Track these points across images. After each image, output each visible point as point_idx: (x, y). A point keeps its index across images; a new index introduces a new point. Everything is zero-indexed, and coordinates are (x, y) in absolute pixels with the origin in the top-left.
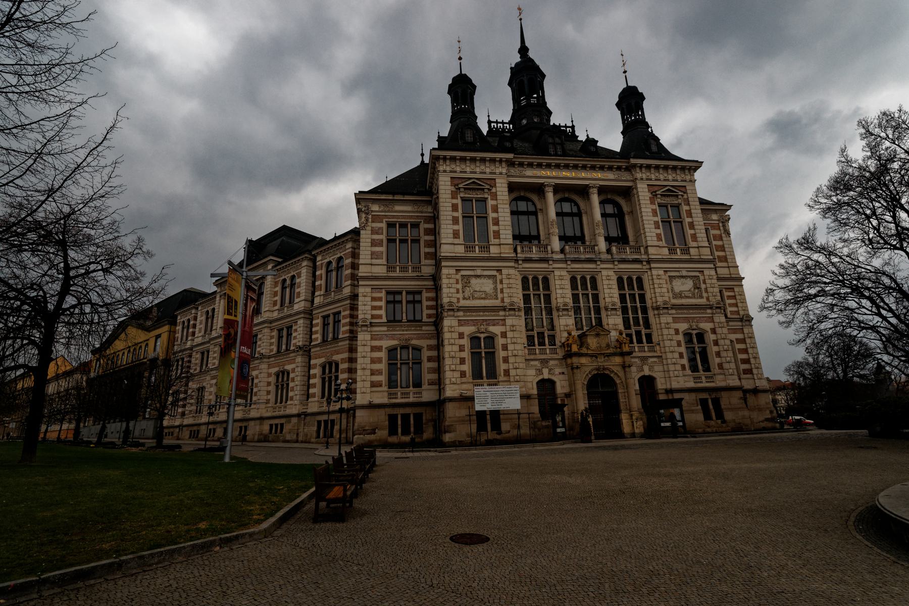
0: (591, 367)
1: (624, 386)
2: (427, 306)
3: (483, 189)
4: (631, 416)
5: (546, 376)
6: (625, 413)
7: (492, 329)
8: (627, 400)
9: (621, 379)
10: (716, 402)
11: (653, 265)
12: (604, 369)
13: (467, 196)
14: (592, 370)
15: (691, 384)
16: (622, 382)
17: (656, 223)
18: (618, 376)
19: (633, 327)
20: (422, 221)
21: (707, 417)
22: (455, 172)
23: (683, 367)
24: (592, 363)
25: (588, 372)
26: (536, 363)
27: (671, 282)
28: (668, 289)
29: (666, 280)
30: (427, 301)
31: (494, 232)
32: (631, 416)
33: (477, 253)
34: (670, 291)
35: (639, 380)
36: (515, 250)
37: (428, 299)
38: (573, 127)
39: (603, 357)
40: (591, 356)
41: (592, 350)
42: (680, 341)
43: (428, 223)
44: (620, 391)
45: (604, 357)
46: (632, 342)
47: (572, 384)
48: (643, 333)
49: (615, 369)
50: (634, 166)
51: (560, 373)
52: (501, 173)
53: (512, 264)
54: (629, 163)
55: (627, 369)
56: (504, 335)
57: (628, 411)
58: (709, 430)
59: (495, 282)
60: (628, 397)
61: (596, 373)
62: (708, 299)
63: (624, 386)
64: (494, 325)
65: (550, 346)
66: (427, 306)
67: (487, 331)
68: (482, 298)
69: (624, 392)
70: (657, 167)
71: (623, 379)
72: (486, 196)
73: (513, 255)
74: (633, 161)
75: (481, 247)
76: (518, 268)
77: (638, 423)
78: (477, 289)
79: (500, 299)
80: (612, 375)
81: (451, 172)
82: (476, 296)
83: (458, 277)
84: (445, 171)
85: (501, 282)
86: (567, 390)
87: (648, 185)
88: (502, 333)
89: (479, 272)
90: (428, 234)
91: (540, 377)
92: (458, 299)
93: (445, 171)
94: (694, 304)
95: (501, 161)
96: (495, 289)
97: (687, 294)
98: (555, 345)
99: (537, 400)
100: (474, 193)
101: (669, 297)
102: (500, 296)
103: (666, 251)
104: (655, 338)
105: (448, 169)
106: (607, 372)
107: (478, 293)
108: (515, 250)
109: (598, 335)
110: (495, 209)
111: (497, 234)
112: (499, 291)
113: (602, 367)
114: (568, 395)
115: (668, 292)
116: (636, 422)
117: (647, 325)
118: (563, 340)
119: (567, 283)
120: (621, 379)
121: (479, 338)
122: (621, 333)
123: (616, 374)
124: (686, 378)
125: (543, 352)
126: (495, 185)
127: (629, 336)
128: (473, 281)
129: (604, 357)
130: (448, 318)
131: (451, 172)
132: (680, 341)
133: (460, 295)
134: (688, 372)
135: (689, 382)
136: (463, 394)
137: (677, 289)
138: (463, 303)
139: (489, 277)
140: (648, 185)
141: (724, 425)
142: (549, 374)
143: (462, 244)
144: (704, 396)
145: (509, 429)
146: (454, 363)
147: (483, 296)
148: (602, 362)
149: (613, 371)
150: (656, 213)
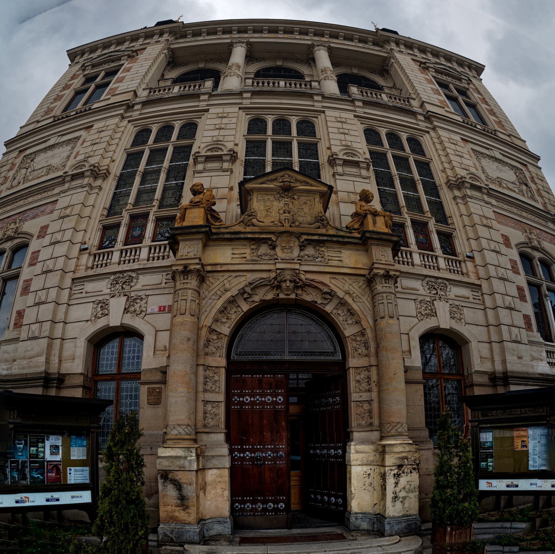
0: (250, 277)
1: (367, 348)
4: (382, 451)
6: (363, 442)
8: (374, 395)
9: (358, 322)
14: (255, 286)
16: (363, 333)
18: (351, 312)
24: (254, 262)
25: (234, 292)
32: (382, 451)
39: (295, 244)
44: (353, 362)
45: (302, 247)
55: (380, 287)
57: (375, 435)
60: (379, 384)
61: (270, 296)
63: (367, 348)
69: (368, 368)
71: (368, 322)
80: (328, 308)
106: (309, 297)
113: (288, 276)
120: (358, 322)
123: (342, 303)
129: (302, 247)
148: (290, 261)
149: (331, 294)
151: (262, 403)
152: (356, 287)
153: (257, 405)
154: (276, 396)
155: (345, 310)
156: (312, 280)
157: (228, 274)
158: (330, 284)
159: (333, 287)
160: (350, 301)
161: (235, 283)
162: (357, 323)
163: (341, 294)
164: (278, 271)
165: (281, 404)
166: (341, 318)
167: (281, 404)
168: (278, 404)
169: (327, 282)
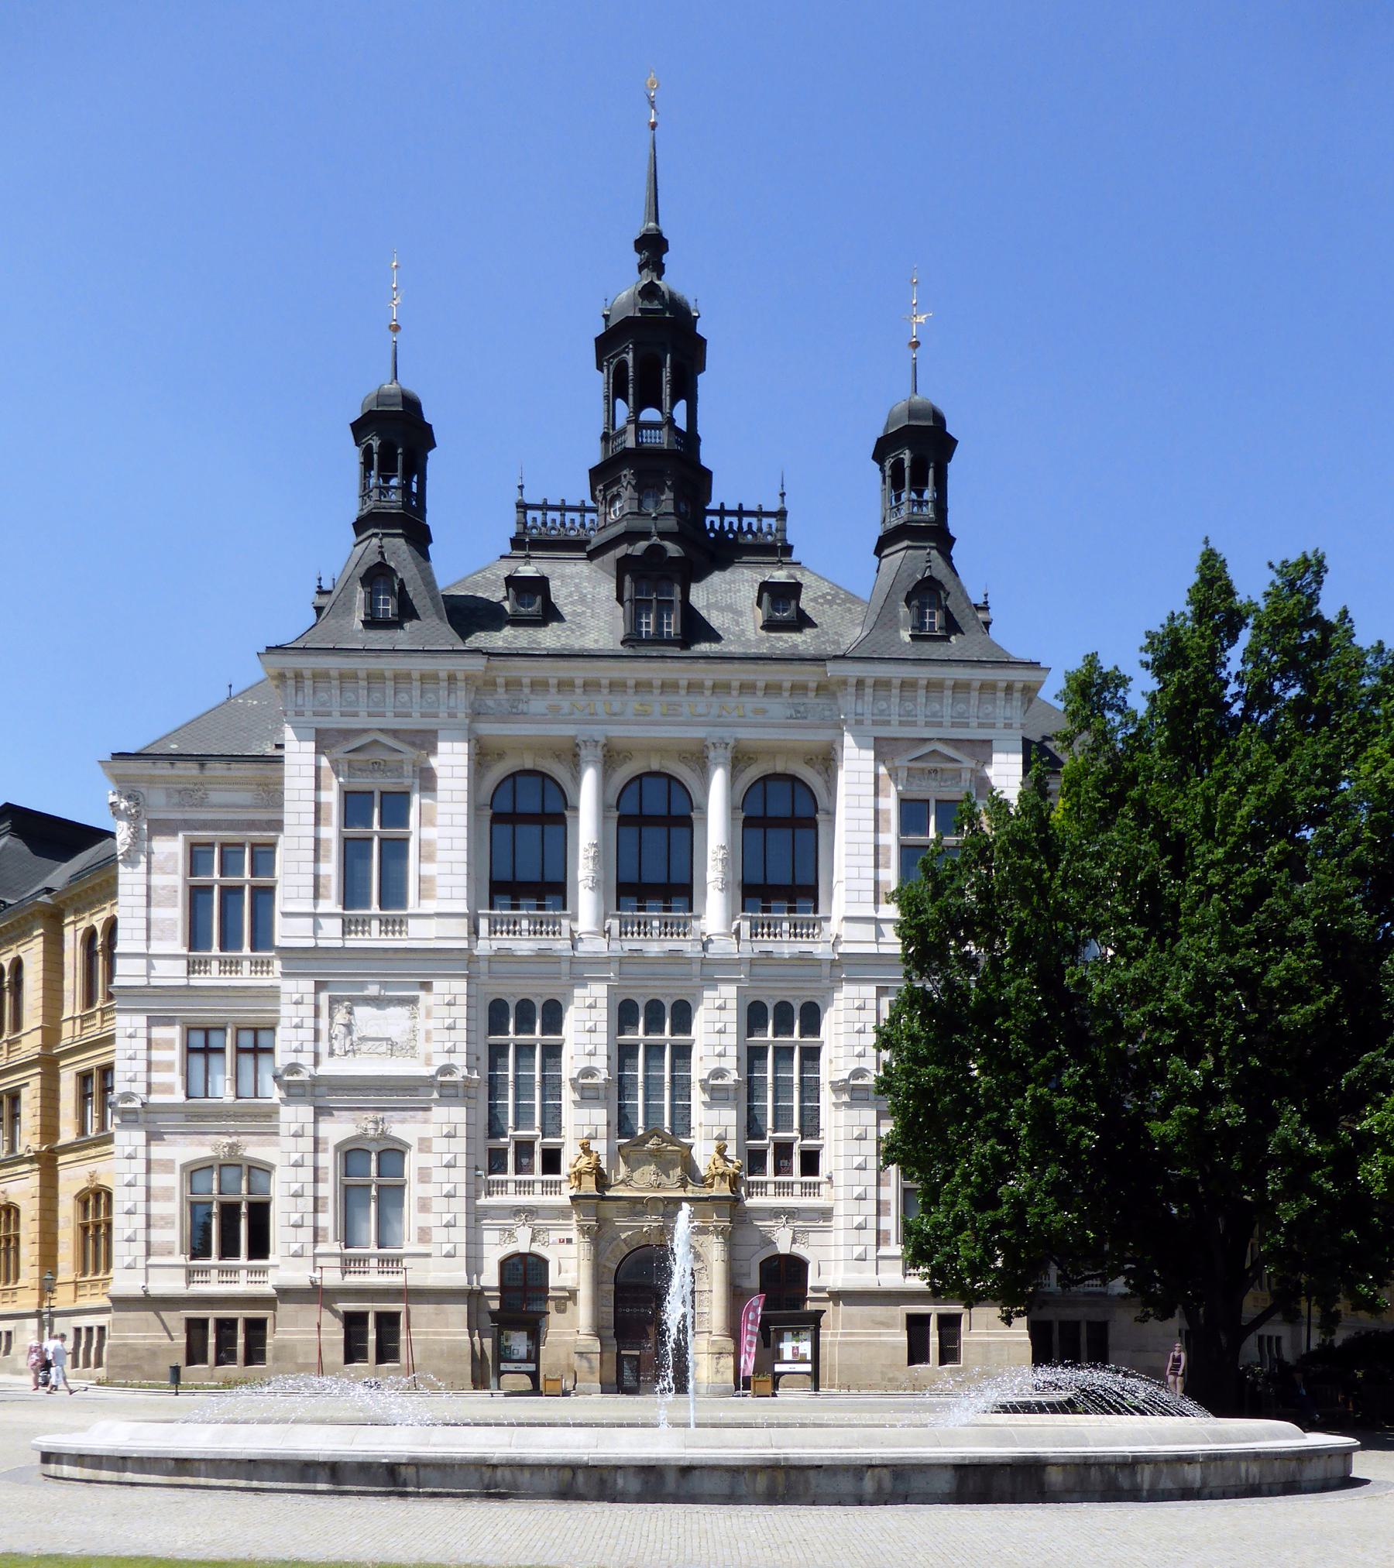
19: (769, 1134)
23: (880, 1238)
33: (374, 938)
36: (474, 931)
51: (561, 1241)
56: (425, 1145)
64: (403, 1121)
67: (384, 1136)
73: (464, 944)
79: (422, 1057)
83: (324, 997)
85: (428, 1015)
88: (422, 1140)
92: (317, 1055)
102: (422, 1047)
104: (825, 1164)
108: (474, 931)
138: (330, 1068)
146: (300, 1208)
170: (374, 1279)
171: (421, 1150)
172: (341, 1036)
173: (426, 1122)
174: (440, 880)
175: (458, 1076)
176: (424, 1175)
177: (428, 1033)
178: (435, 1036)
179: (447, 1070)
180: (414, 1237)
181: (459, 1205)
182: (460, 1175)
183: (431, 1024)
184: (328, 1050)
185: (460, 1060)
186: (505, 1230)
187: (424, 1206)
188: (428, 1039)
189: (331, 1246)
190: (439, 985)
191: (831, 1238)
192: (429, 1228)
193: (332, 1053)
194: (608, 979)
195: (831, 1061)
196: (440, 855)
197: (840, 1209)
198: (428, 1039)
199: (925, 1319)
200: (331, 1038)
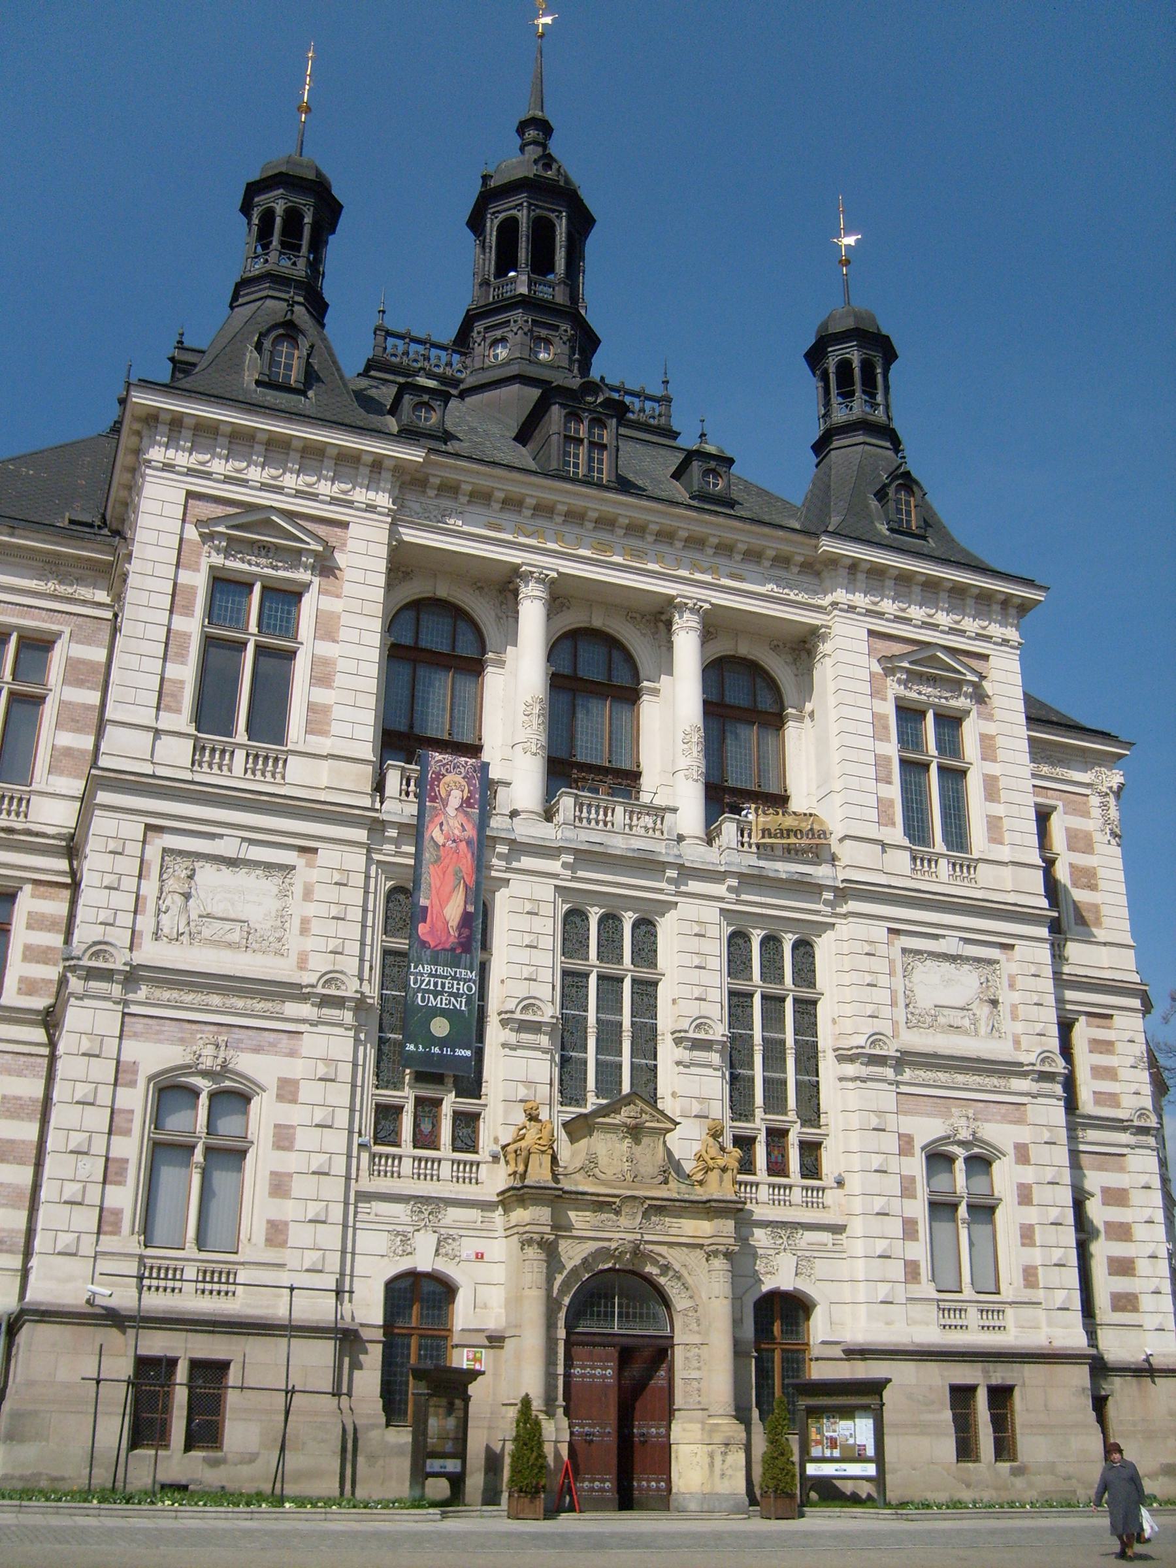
2: (28, 948)
3: (300, 552)
5: (424, 1262)
7: (247, 1063)
10: (1001, 1396)
11: (853, 906)
12: (637, 1251)
13: (230, 564)
15: (930, 1335)
17: (881, 762)
19: (759, 1113)
20: (67, 631)
21: (966, 1450)
22: (207, 475)
23: (912, 1271)
26: (399, 1211)
27: (907, 973)
28: (893, 993)
29: (891, 962)
30: (29, 927)
31: (311, 707)
34: (901, 1002)
35: (756, 1304)
36: (379, 787)
37: (36, 922)
38: (666, 400)
40: (600, 1205)
41: (604, 1183)
42: (912, 1179)
43: (88, 641)
46: (747, 1166)
47: (514, 1301)
48: (793, 1138)
49: (675, 1257)
50: (833, 561)
52: (371, 508)
53: (361, 835)
54: (816, 547)
56: (288, 1091)
58: (966, 1495)
59: (284, 894)
62: (1017, 1043)
64: (257, 1050)
65: (455, 1149)
66: (28, 948)
67: (224, 1071)
68: (229, 945)
70: (904, 580)
72: (303, 575)
73: (367, 802)
74: (829, 546)
75: (256, 756)
76: (380, 851)
77: (730, 1459)
78: (218, 911)
79: (293, 959)
80: (662, 1280)
81: (191, 472)
82: (206, 933)
83: (153, 853)
84: (168, 467)
85: (308, 895)
86: (494, 1320)
87: (871, 633)
89: (227, 847)
90: (80, 683)
91: (404, 1265)
93: (168, 467)
94: (973, 1055)
95: (377, 464)
96: (282, 916)
97: (956, 1018)
98: (473, 1148)
99: (379, 1348)
100: (263, 561)
101: (895, 1023)
102: (295, 943)
103: (901, 861)
104: (830, 1163)
105: (182, 459)
107: (218, 924)
108: (379, 787)
109: (635, 1132)
110: (327, 629)
111: (318, 719)
112: (296, 923)
114: (495, 1341)
115: (894, 1004)
116: (724, 1454)
117: (811, 1111)
118: (506, 1137)
119: (548, 928)
121: (195, 1093)
122: (716, 1134)
124: (917, 1310)
125: (426, 1169)
126: (344, 545)
127: (744, 1143)
128: (207, 874)
130: (87, 1002)
131: (191, 472)
132: (912, 1179)
133: (145, 923)
134: (927, 1289)
135: (927, 1324)
136: (99, 1301)
137: (925, 999)
138: (151, 953)
139: (269, 867)
140: (871, 633)
141: (1019, 1482)
142: (437, 1253)
143: (187, 735)
144: (965, 1374)
145: (255, 1449)
146: (82, 1174)
147: (235, 937)
150: (886, 728)
151: (593, 1376)
152: (693, 1258)
153: (587, 1377)
154: (606, 1368)
155: (680, 1284)
156: (651, 1251)
157: (570, 1241)
158: (667, 1256)
159: (670, 1259)
160: (685, 1274)
161: (579, 1250)
162: (691, 1297)
163: (677, 1266)
164: (621, 1241)
165: (611, 1378)
166: (674, 1291)
167: (611, 1378)
168: (607, 1378)
169: (665, 1253)
170: (191, 1302)
171: (280, 1097)
172: (174, 910)
173: (292, 1054)
174: (337, 712)
175: (350, 989)
176: (284, 1138)
177: (305, 921)
178: (316, 927)
179: (330, 979)
180: (260, 1236)
181: (334, 1189)
182: (337, 1141)
183: (311, 909)
184: (152, 928)
185: (350, 965)
186: (398, 1234)
187: (279, 1186)
188: (304, 930)
189: (128, 1241)
190: (328, 856)
191: (842, 1269)
192: (286, 1224)
193: (156, 936)
194: (555, 876)
195: (834, 1021)
196: (339, 680)
197: (857, 1227)
198: (304, 930)
199: (972, 1389)
200: (159, 912)
